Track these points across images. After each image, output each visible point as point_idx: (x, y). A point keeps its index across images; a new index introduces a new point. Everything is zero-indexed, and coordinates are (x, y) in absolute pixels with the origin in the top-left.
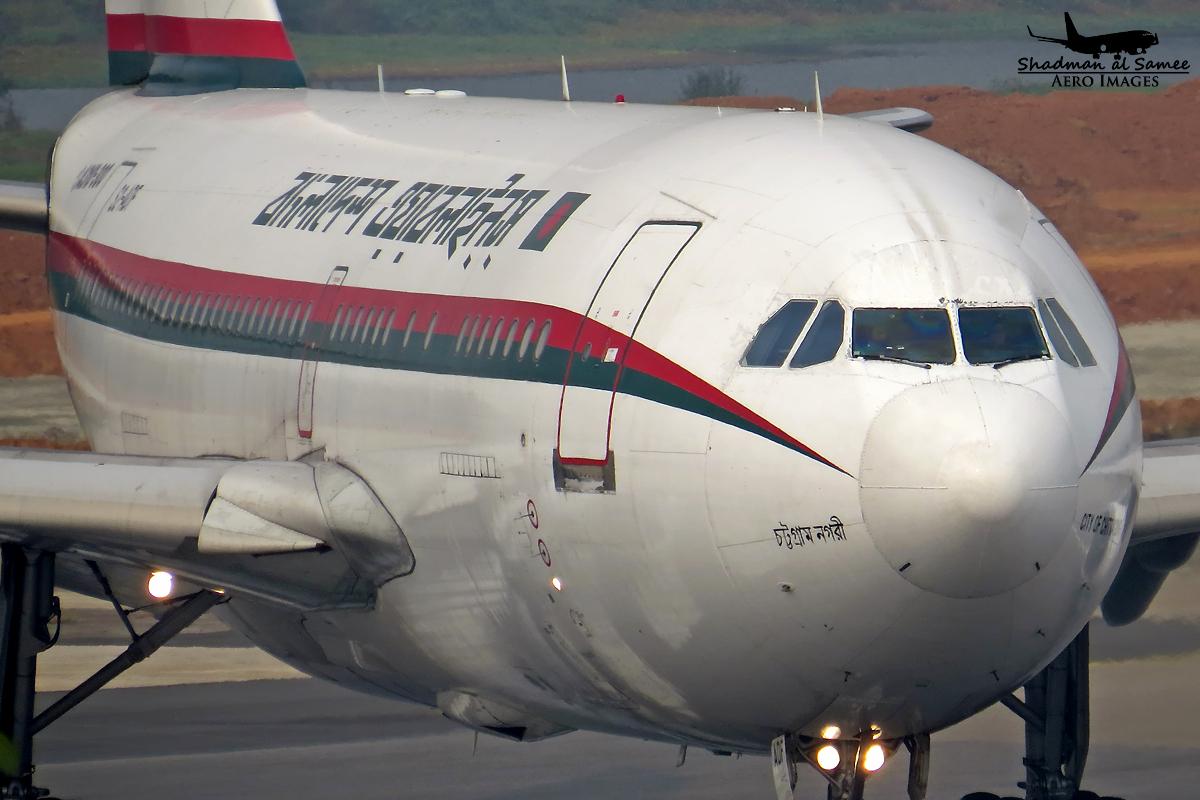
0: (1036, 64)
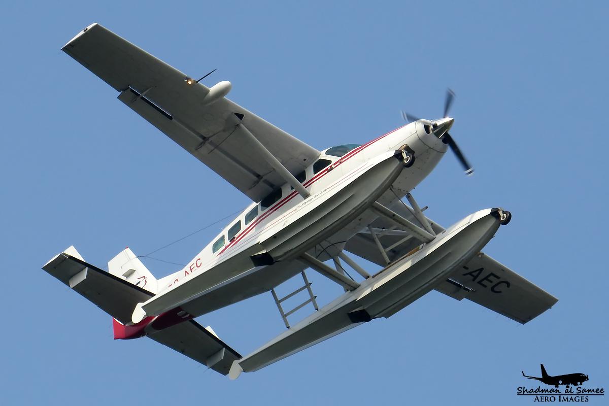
0: (526, 390)
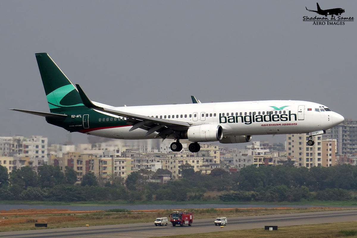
0: (308, 18)
